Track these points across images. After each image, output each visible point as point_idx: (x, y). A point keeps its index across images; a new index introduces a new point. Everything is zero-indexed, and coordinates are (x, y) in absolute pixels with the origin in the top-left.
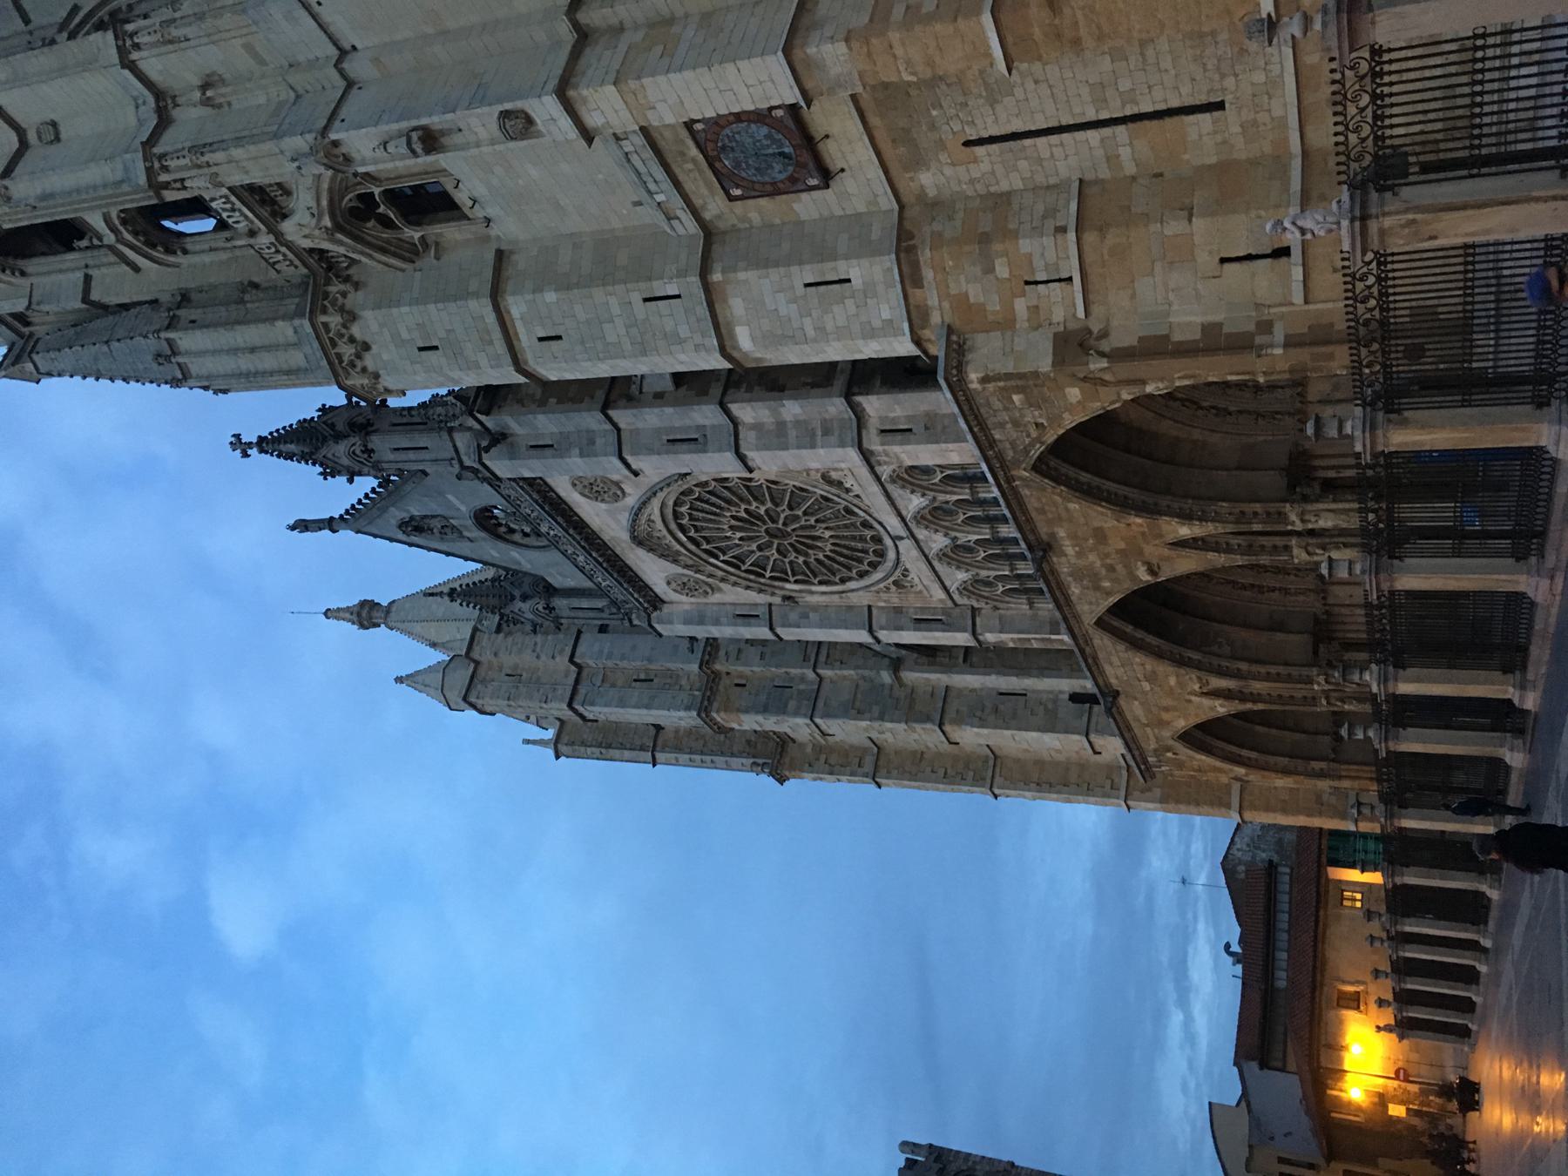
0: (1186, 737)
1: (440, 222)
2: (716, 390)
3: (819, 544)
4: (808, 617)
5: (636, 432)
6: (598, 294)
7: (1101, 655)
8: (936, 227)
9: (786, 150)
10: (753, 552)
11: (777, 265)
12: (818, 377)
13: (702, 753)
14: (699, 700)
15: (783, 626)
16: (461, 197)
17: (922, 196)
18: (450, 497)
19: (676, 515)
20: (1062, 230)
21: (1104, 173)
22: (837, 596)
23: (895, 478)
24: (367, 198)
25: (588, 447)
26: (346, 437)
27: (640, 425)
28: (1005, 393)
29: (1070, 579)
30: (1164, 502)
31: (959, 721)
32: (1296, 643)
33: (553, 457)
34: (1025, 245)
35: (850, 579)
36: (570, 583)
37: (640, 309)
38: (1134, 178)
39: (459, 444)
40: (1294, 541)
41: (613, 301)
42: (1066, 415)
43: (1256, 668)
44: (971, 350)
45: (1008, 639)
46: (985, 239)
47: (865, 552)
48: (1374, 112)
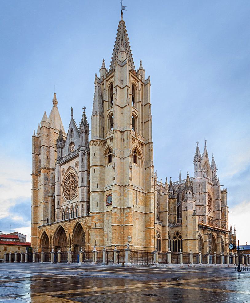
0: (44, 232)
1: (108, 160)
6: (99, 178)
12: (89, 198)
14: (45, 167)
15: (58, 184)
17: (104, 214)
20: (100, 227)
21: (104, 231)
23: (77, 204)
24: (111, 153)
25: (83, 167)
28: (86, 221)
30: (74, 233)
31: (44, 204)
32: (57, 244)
34: (99, 224)
36: (63, 152)
39: (83, 147)
41: (98, 180)
46: (100, 220)
47: (68, 197)
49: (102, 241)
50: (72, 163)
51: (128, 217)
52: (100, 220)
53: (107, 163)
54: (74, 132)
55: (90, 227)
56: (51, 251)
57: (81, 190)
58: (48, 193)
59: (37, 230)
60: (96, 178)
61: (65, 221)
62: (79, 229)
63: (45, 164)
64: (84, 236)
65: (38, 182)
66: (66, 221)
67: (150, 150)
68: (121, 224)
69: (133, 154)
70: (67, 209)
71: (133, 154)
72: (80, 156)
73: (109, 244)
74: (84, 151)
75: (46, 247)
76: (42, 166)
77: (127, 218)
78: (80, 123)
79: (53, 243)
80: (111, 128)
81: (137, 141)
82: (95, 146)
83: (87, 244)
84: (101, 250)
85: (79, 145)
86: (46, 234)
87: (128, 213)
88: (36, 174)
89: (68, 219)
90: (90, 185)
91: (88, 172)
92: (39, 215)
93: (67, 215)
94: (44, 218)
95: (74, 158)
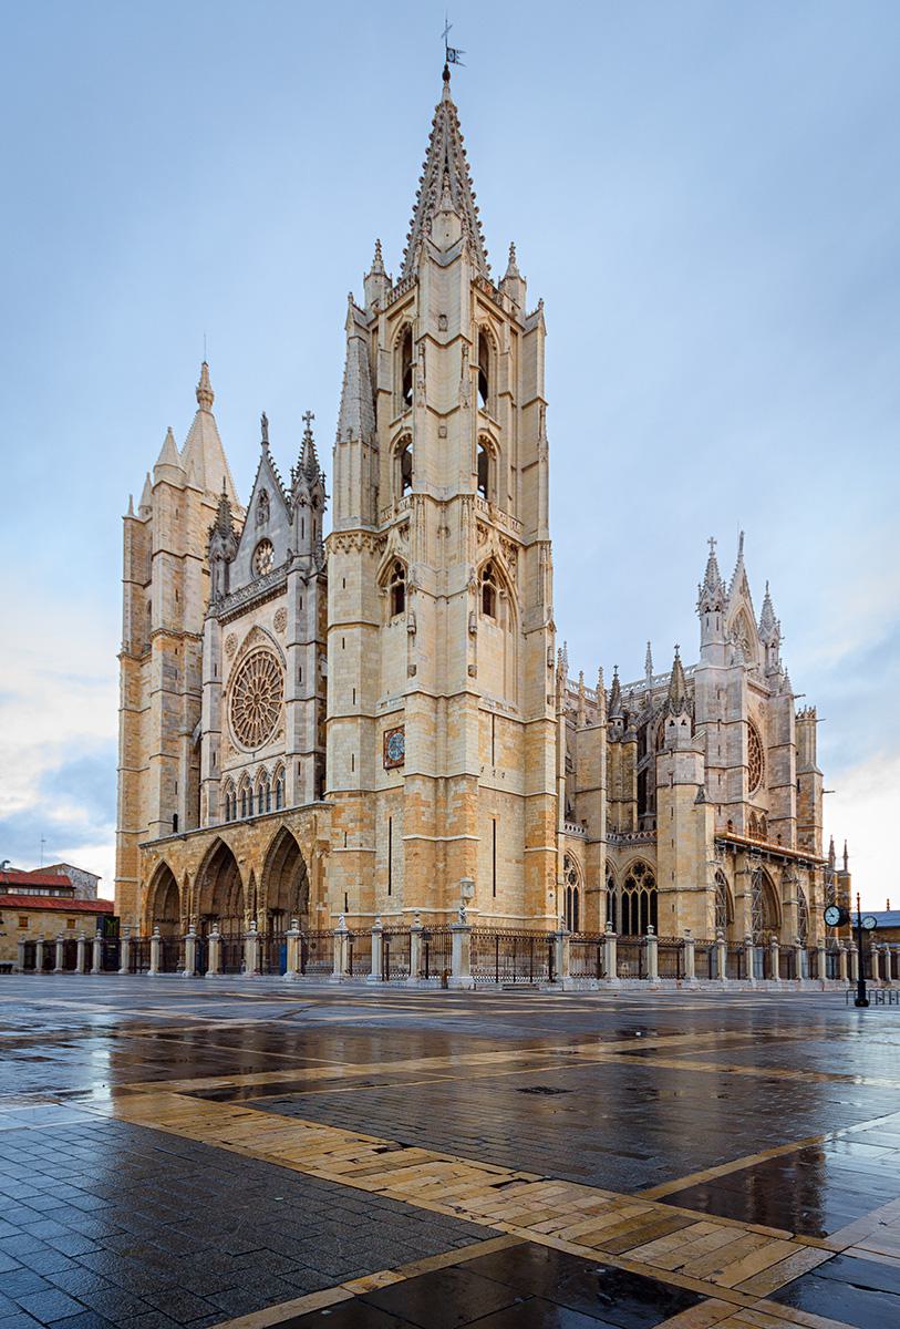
0: (164, 864)
2: (320, 695)
6: (358, 670)
12: (322, 741)
16: (398, 618)
17: (377, 799)
21: (377, 859)
23: (280, 761)
24: (402, 577)
25: (301, 628)
28: (310, 822)
30: (269, 869)
31: (163, 763)
32: (208, 908)
34: (357, 833)
36: (232, 575)
37: (351, 687)
43: (198, 894)
45: (205, 793)
46: (362, 820)
49: (370, 896)
51: (463, 808)
52: (362, 820)
53: (388, 614)
54: (273, 504)
55: (325, 847)
56: (187, 931)
58: (177, 723)
59: (136, 854)
60: (348, 668)
61: (236, 825)
62: (286, 851)
63: (169, 619)
64: (304, 877)
65: (144, 684)
66: (241, 824)
67: (542, 569)
68: (436, 835)
69: (479, 584)
70: (246, 779)
71: (479, 584)
72: (291, 589)
73: (392, 908)
74: (308, 572)
75: (168, 917)
76: (157, 624)
77: (457, 813)
78: (293, 471)
79: (194, 902)
80: (404, 488)
81: (497, 534)
82: (347, 552)
83: (314, 907)
84: (365, 929)
85: (289, 550)
86: (169, 869)
87: (463, 796)
88: (135, 655)
89: (247, 817)
90: (325, 695)
91: (322, 647)
92: (144, 802)
93: (244, 802)
95: (269, 596)
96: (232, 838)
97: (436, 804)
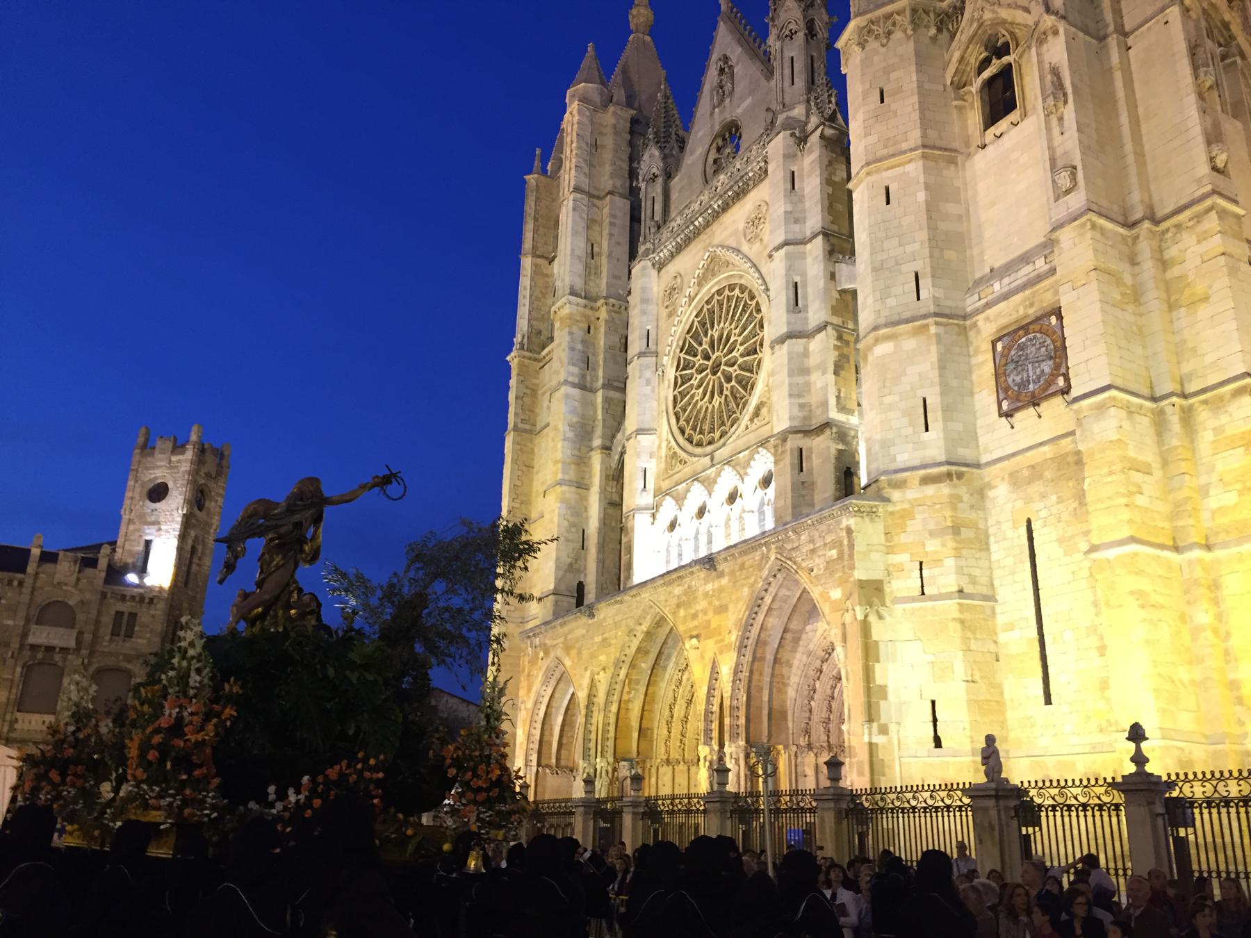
3: (706, 398)
4: (647, 385)
5: (803, 256)
6: (923, 235)
7: (623, 607)
8: (965, 499)
9: (1031, 386)
10: (701, 344)
11: (941, 376)
13: (531, 296)
15: (641, 365)
16: (1003, 125)
17: (990, 486)
18: (749, 101)
19: (732, 288)
21: (1001, 620)
22: (664, 408)
24: (1003, 50)
25: (794, 217)
26: (805, 17)
27: (809, 260)
28: (837, 544)
29: (686, 586)
33: (785, 190)
34: (950, 563)
35: (678, 419)
36: (674, 196)
38: (996, 642)
40: (716, 748)
41: (916, 246)
42: (820, 588)
44: (872, 520)
46: (956, 530)
48: (1073, 805)
50: (726, 229)
57: (790, 359)
65: (544, 394)
91: (833, 240)
94: (558, 581)
96: (673, 602)
97: (1165, 463)
